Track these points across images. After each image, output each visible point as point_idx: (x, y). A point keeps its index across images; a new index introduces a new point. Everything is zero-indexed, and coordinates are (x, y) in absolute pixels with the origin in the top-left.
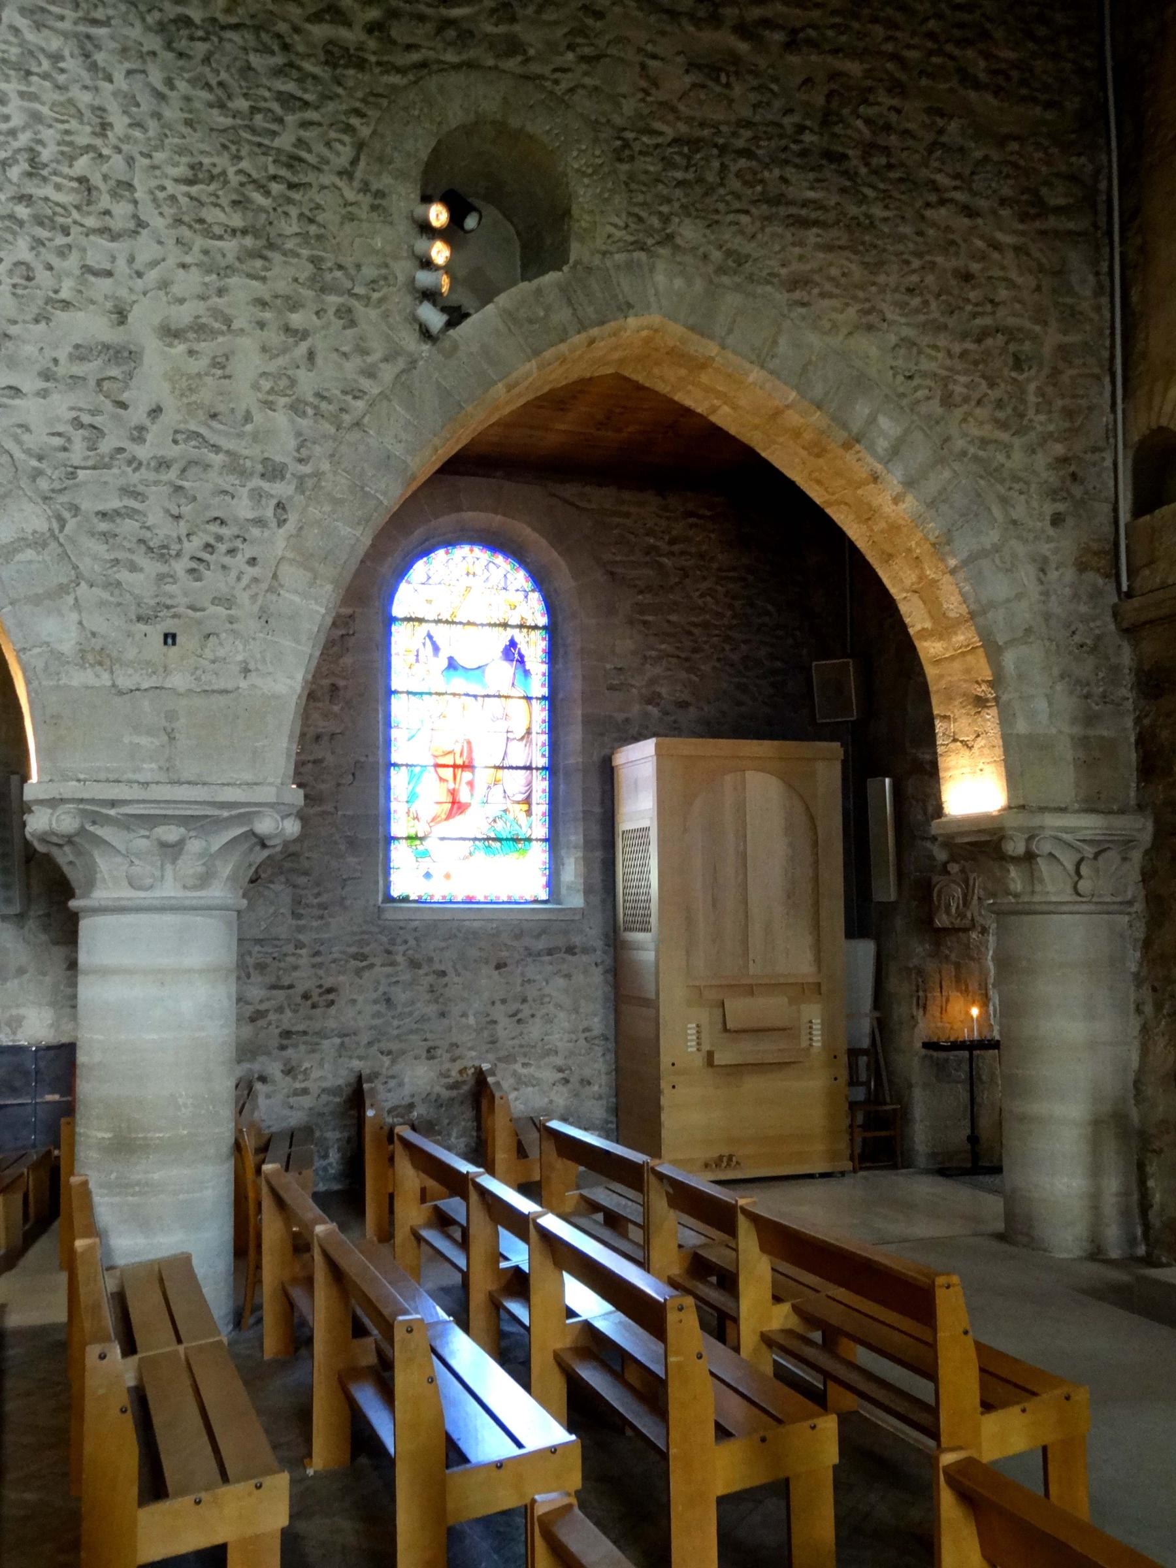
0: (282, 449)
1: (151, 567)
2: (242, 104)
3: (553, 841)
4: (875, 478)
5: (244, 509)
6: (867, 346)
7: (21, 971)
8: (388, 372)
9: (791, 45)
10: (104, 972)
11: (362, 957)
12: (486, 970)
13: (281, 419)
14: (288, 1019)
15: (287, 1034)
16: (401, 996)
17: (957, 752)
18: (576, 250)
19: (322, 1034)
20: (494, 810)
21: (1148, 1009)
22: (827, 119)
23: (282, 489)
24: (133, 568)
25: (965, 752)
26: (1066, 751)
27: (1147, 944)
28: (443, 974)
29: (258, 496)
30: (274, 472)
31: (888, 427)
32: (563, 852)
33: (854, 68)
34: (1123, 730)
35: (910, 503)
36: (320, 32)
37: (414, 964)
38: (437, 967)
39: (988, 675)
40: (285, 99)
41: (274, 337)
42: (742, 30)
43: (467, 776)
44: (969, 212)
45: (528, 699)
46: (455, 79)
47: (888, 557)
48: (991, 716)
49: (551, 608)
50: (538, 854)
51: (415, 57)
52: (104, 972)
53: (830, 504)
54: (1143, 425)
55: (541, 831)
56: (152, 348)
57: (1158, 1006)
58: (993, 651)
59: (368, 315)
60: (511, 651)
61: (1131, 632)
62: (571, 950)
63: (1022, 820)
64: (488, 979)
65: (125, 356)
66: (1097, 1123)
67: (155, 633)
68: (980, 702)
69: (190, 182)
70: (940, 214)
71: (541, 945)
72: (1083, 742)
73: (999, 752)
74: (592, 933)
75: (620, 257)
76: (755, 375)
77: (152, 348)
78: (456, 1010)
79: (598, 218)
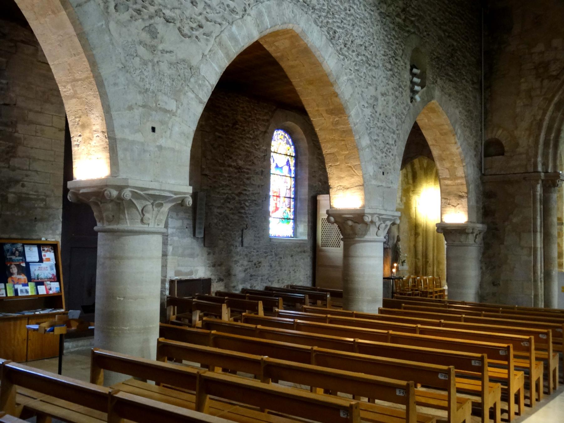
0: (394, 127)
1: (381, 155)
2: (389, 36)
3: (295, 220)
4: (456, 143)
5: (391, 142)
6: (457, 111)
7: (198, 255)
8: (407, 108)
9: (449, 37)
10: (368, 257)
11: (266, 253)
12: (289, 257)
13: (394, 118)
14: (251, 271)
15: (251, 276)
16: (274, 265)
17: (450, 207)
18: (427, 83)
19: (258, 276)
20: (283, 210)
21: (484, 268)
22: (452, 56)
23: (395, 137)
24: (379, 155)
26: (475, 209)
27: (484, 254)
28: (281, 258)
29: (393, 138)
30: (394, 133)
31: (459, 131)
32: (298, 223)
33: (455, 44)
34: (481, 206)
35: (460, 150)
36: (398, 19)
37: (276, 255)
38: (280, 256)
39: (466, 190)
40: (394, 36)
41: (394, 97)
42: (444, 31)
43: (278, 199)
44: (467, 81)
45: (291, 177)
46: (413, 36)
47: (442, 159)
49: (296, 151)
50: (291, 223)
51: (407, 29)
52: (368, 257)
53: (433, 145)
54: (490, 136)
55: (292, 217)
56: (379, 96)
57: (487, 268)
58: (468, 184)
59: (404, 93)
60: (288, 163)
61: (483, 183)
62: (304, 252)
63: (471, 225)
64: (289, 260)
65: (376, 99)
66: (476, 294)
67: (381, 171)
68: (461, 197)
69: (384, 55)
70: (464, 81)
71: (299, 250)
72: (477, 207)
73: (466, 209)
74: (308, 248)
75: (432, 85)
76: (445, 116)
77: (379, 96)
78: (283, 269)
79: (430, 75)
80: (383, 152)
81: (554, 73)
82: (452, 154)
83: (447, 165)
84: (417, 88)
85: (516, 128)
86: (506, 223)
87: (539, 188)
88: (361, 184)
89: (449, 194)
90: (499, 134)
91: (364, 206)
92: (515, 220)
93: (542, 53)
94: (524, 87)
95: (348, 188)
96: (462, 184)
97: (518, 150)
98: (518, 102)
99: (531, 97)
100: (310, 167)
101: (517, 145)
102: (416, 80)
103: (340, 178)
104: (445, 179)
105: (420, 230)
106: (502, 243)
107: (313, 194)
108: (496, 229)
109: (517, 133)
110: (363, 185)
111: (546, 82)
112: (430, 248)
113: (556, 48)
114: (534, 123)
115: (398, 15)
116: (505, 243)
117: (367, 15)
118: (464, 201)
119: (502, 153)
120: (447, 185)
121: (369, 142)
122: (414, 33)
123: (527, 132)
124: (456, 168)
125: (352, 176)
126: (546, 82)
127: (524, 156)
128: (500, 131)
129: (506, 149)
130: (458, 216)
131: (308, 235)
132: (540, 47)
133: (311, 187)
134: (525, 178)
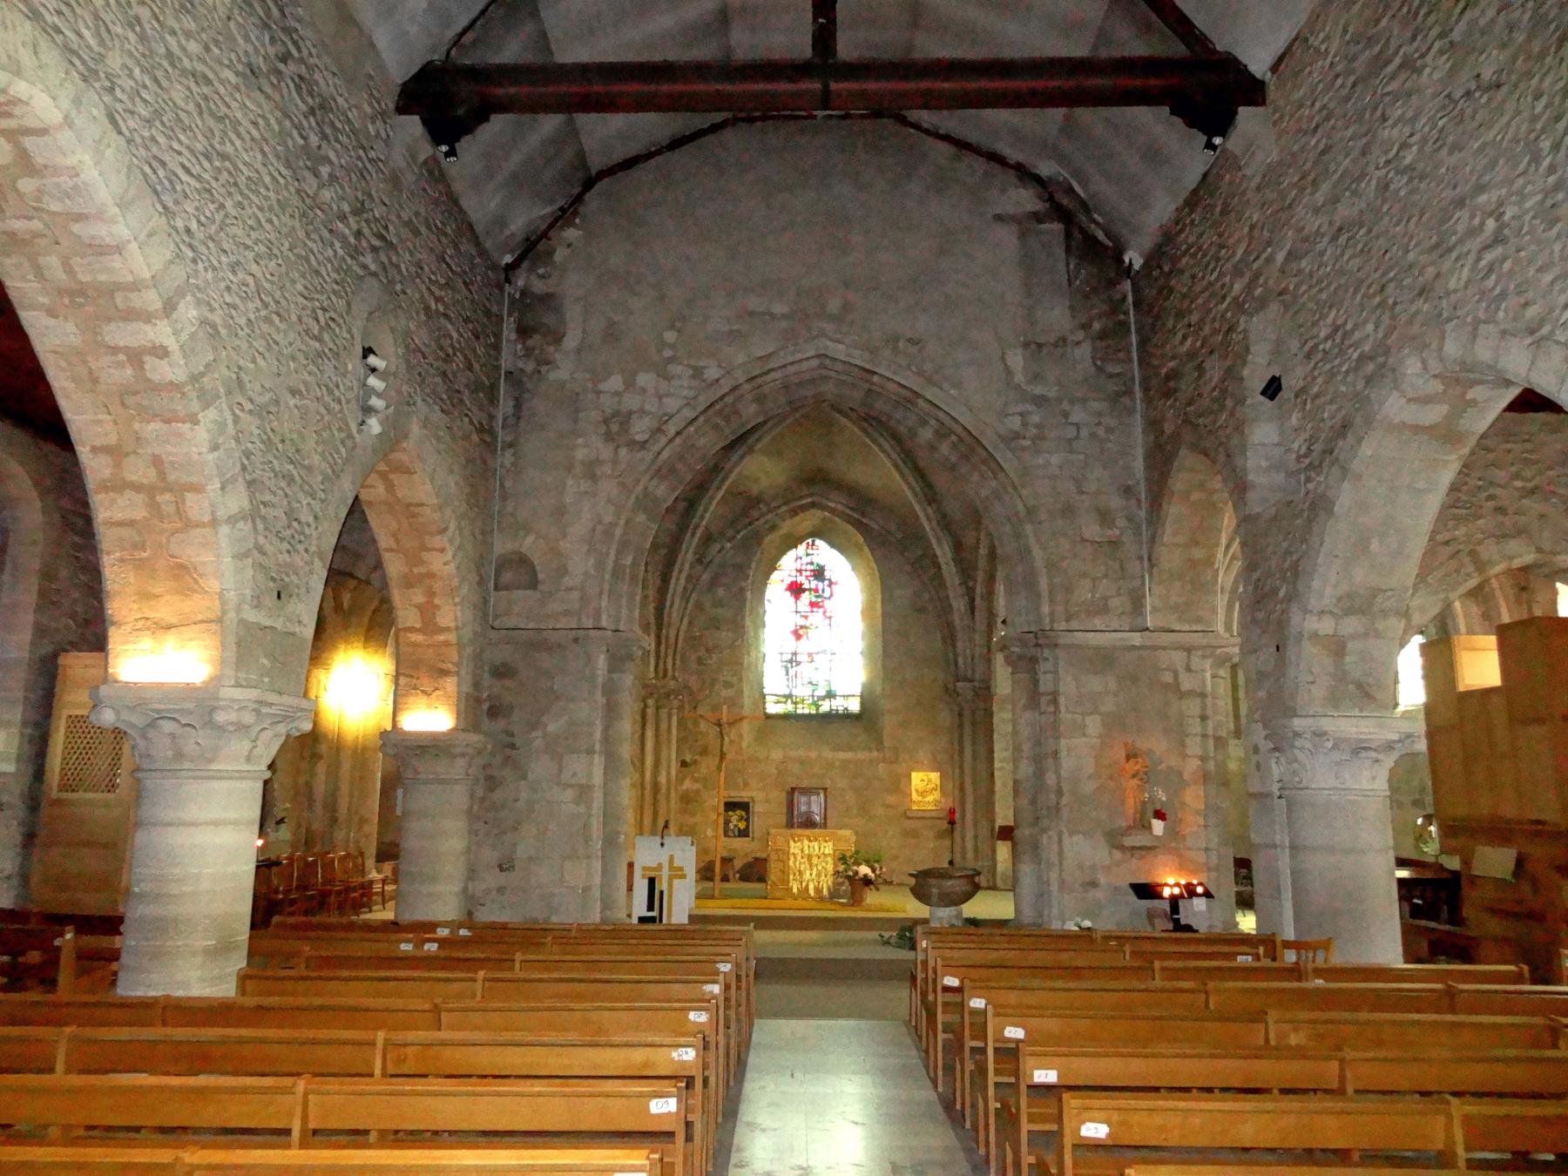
25: (423, 700)
30: (313, 495)
35: (451, 568)
48: (450, 684)
53: (391, 550)
58: (461, 646)
68: (444, 673)
80: (282, 539)
81: (638, 438)
82: (431, 575)
83: (419, 597)
84: (375, 402)
85: (564, 535)
86: (534, 734)
87: (602, 661)
88: (211, 616)
89: (416, 665)
90: (528, 544)
91: (216, 680)
92: (552, 728)
93: (618, 394)
94: (580, 454)
95: (169, 627)
96: (447, 644)
97: (566, 579)
98: (570, 482)
99: (593, 478)
100: (48, 575)
101: (563, 571)
102: (372, 381)
103: (146, 596)
104: (411, 629)
105: (323, 748)
106: (524, 778)
107: (46, 649)
108: (512, 746)
109: (564, 545)
110: (220, 620)
111: (623, 452)
112: (344, 788)
113: (644, 390)
114: (599, 528)
115: (343, 218)
116: (530, 776)
117: (267, 179)
118: (450, 684)
119: (533, 584)
120: (415, 645)
121: (246, 504)
122: (375, 274)
123: (586, 548)
124: (438, 607)
125: (186, 591)
126: (623, 452)
127: (576, 594)
128: (530, 539)
129: (540, 576)
130: (432, 717)
131: (19, 759)
132: (615, 382)
133: (40, 631)
134: (576, 640)
